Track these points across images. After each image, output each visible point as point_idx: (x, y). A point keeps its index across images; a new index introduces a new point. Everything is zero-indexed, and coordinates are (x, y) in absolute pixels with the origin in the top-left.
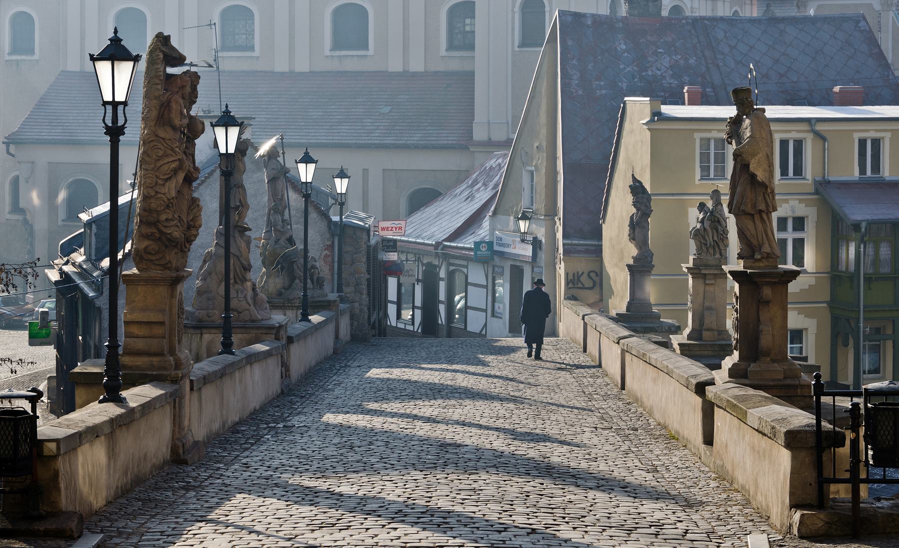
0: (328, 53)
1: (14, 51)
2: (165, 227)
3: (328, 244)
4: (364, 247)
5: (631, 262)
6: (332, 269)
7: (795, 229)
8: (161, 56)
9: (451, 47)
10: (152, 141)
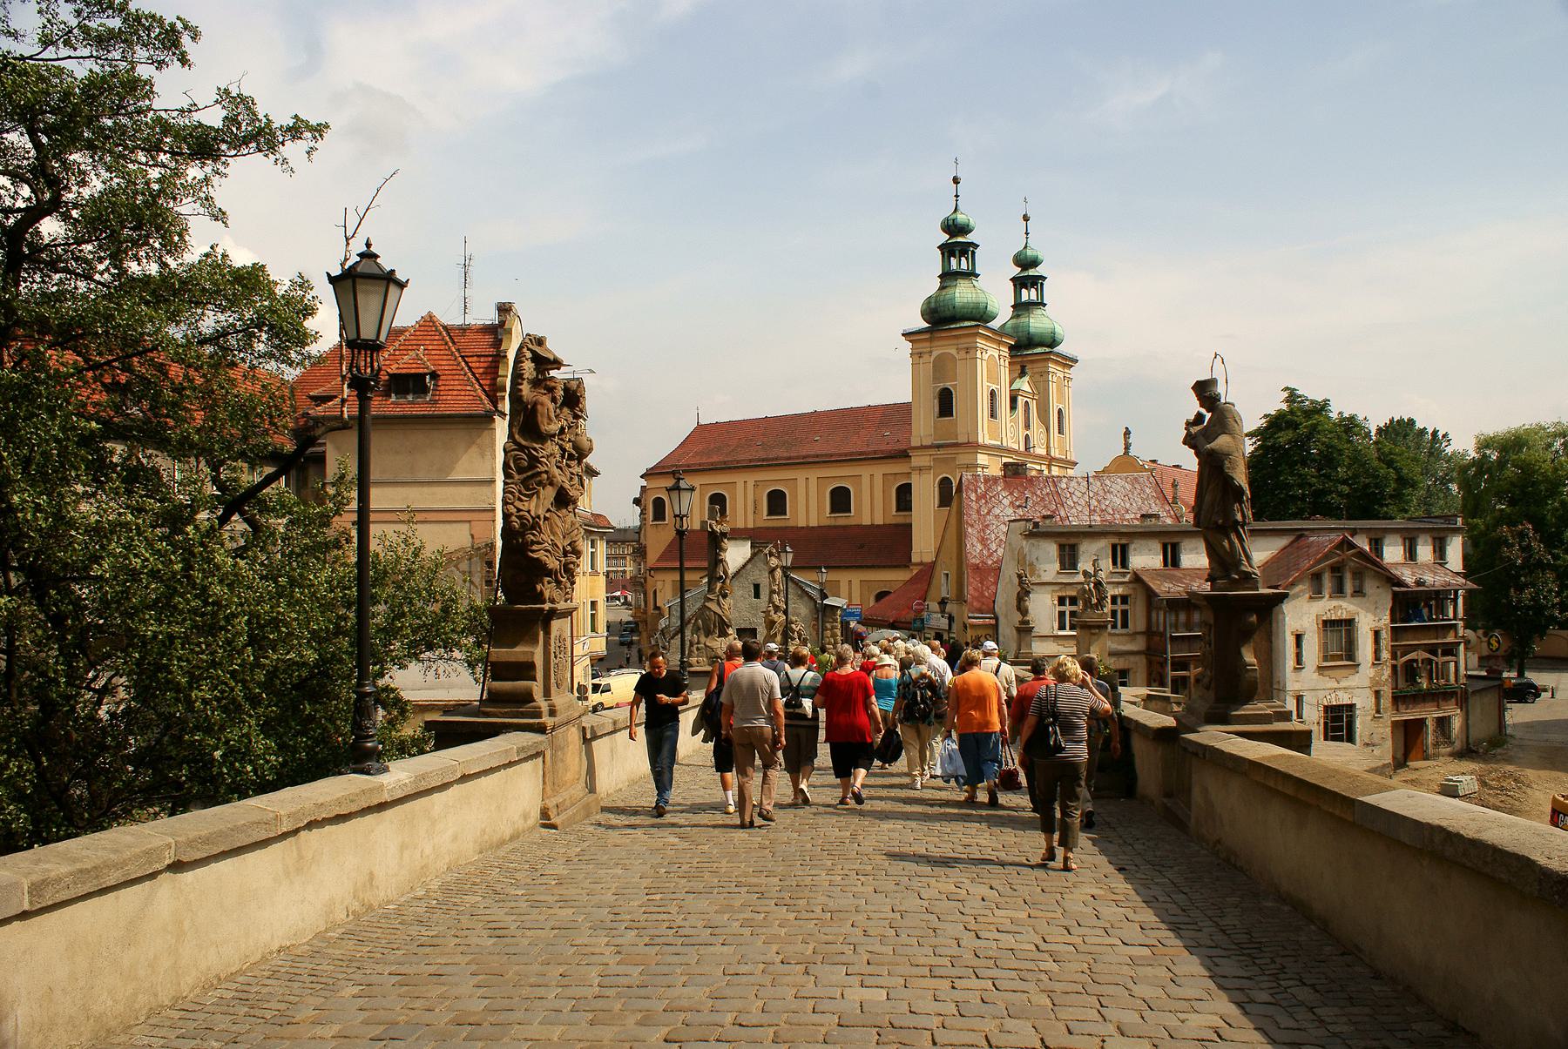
1: (655, 519)
2: (533, 551)
5: (1018, 625)
6: (817, 634)
7: (1122, 603)
8: (529, 355)
10: (513, 450)
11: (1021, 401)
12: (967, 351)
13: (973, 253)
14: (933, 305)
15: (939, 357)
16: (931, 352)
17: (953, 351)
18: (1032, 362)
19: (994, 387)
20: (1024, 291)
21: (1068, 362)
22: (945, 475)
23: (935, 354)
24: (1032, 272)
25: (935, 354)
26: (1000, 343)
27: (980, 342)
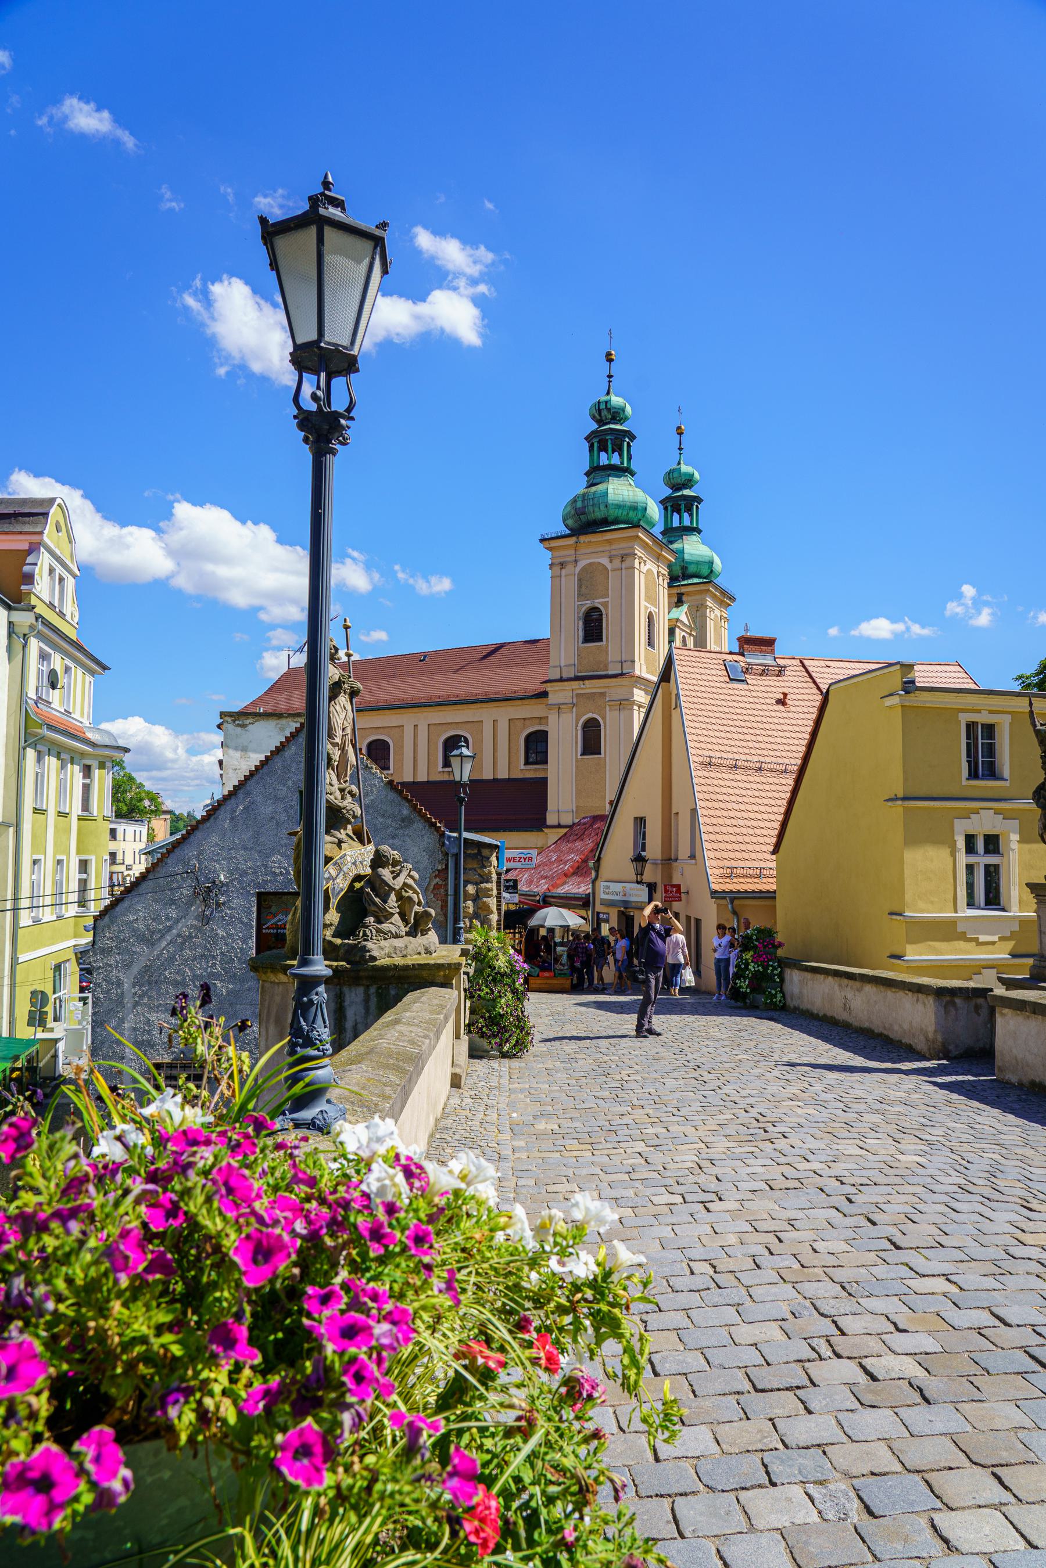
0: (441, 770)
3: (440, 868)
4: (494, 876)
6: (444, 906)
9: (527, 763)
11: (678, 633)
12: (623, 558)
13: (629, 445)
14: (579, 504)
15: (584, 569)
16: (576, 561)
17: (605, 561)
18: (689, 594)
19: (652, 609)
20: (676, 516)
21: (726, 599)
22: (590, 715)
23: (582, 564)
24: (686, 492)
25: (582, 564)
26: (658, 558)
27: (639, 552)
